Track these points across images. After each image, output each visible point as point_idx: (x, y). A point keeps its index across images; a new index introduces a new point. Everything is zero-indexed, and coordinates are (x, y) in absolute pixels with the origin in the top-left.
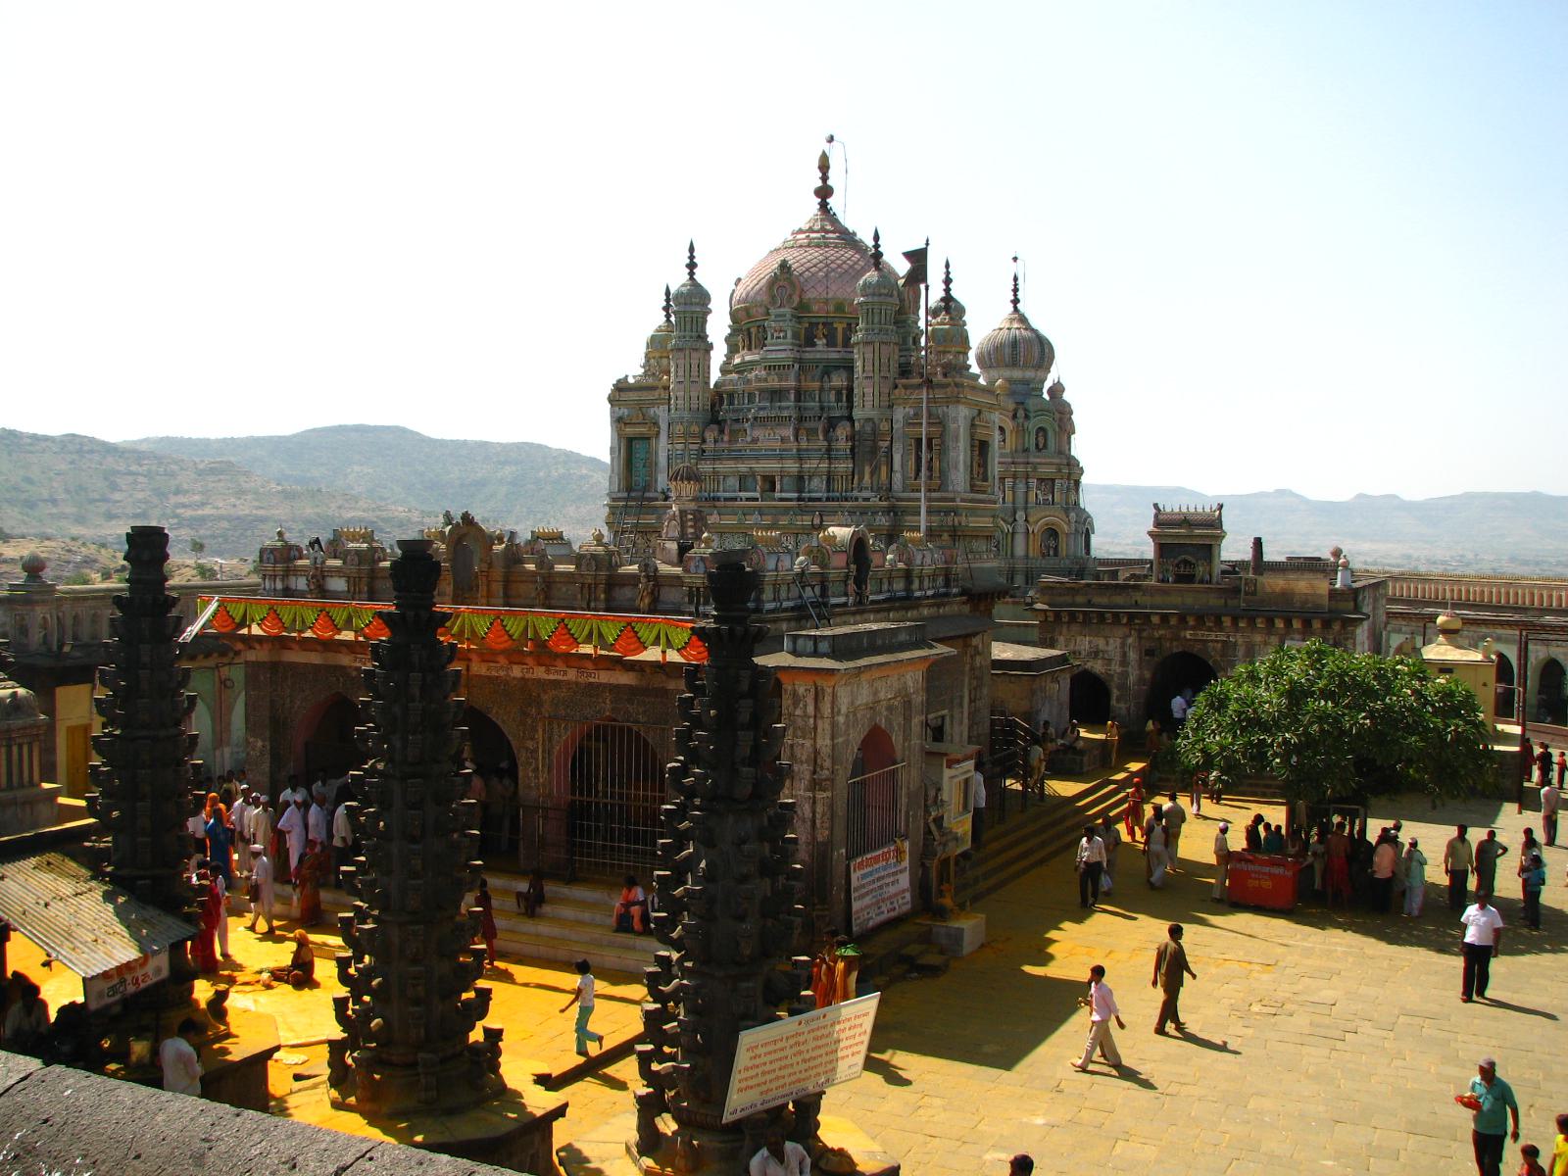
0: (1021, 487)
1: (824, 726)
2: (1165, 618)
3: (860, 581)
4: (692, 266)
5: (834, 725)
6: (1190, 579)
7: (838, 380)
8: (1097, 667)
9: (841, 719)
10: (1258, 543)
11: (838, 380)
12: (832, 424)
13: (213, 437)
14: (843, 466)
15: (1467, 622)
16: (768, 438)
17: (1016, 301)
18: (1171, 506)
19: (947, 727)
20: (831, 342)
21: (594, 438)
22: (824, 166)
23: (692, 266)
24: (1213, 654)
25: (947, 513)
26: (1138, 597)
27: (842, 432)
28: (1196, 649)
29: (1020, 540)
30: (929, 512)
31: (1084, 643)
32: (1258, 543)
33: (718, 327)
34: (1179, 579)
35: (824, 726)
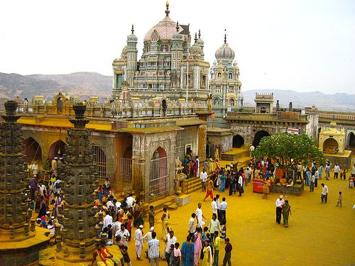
0: (225, 88)
1: (142, 146)
2: (258, 122)
3: (164, 110)
4: (133, 31)
5: (145, 146)
6: (265, 112)
7: (168, 60)
8: (241, 134)
9: (148, 145)
10: (291, 103)
11: (168, 60)
12: (166, 71)
13: (23, 73)
14: (169, 81)
15: (340, 124)
16: (150, 74)
17: (225, 41)
18: (260, 93)
19: (191, 149)
20: (167, 50)
21: (109, 72)
22: (167, 6)
23: (133, 31)
24: (270, 131)
25: (194, 93)
26: (251, 116)
27: (169, 72)
28: (265, 130)
29: (224, 101)
30: (189, 93)
31: (237, 128)
32: (291, 103)
33: (140, 47)
34: (262, 112)
35: (142, 146)
